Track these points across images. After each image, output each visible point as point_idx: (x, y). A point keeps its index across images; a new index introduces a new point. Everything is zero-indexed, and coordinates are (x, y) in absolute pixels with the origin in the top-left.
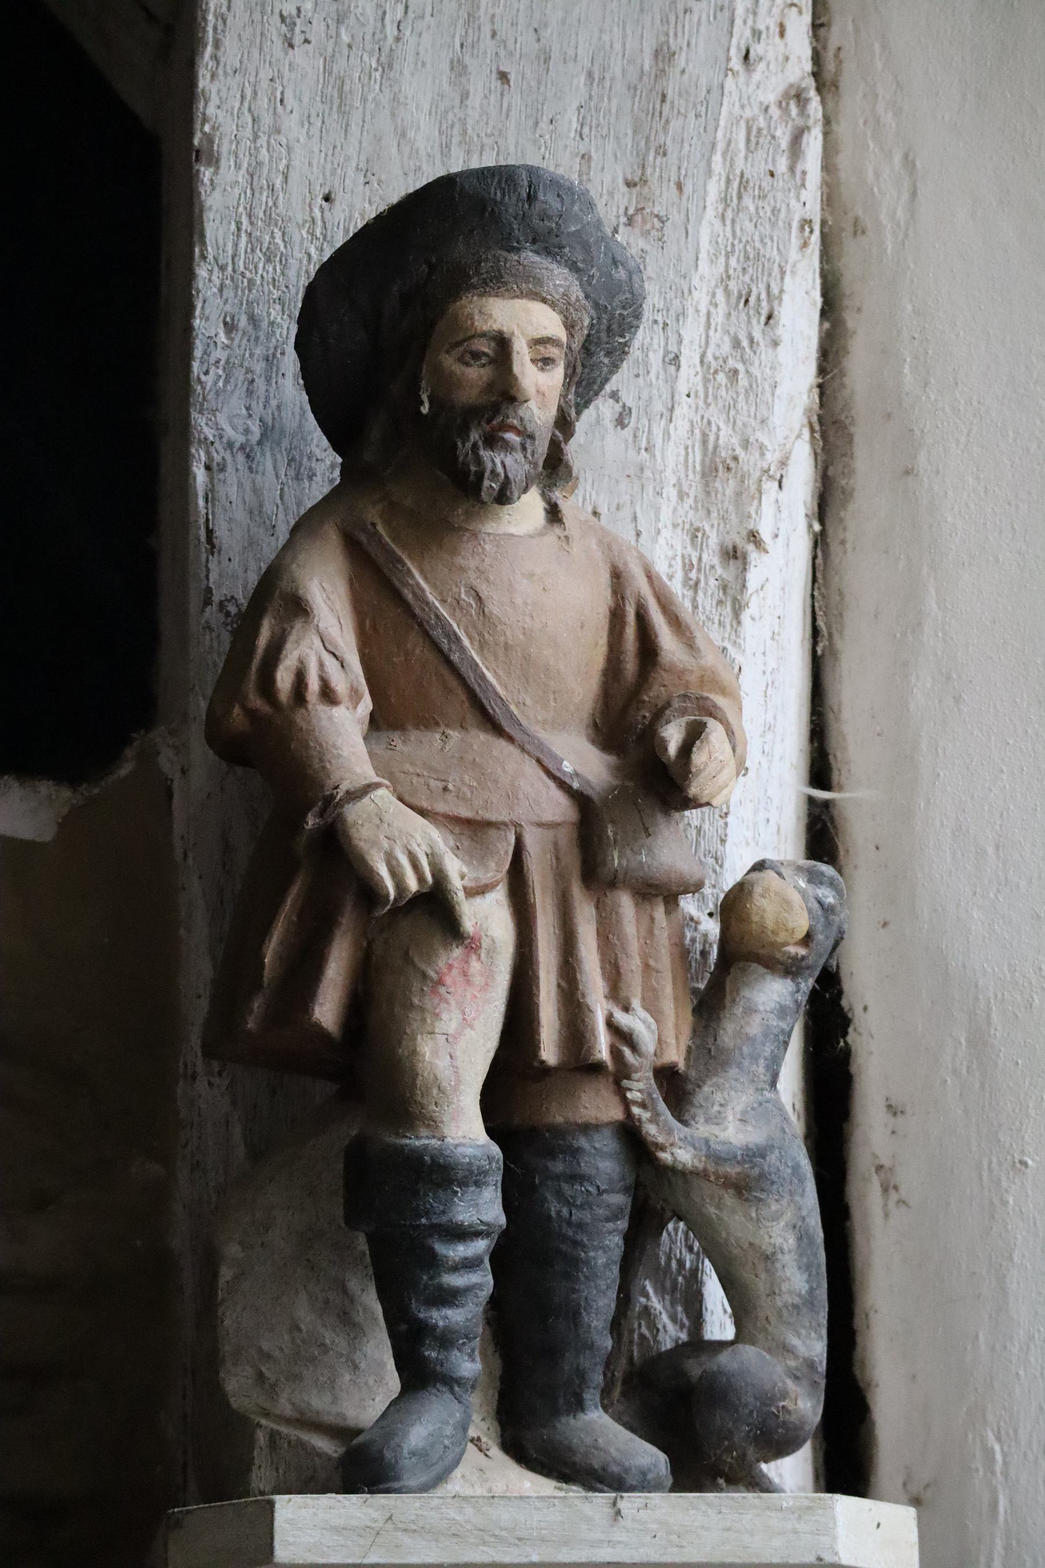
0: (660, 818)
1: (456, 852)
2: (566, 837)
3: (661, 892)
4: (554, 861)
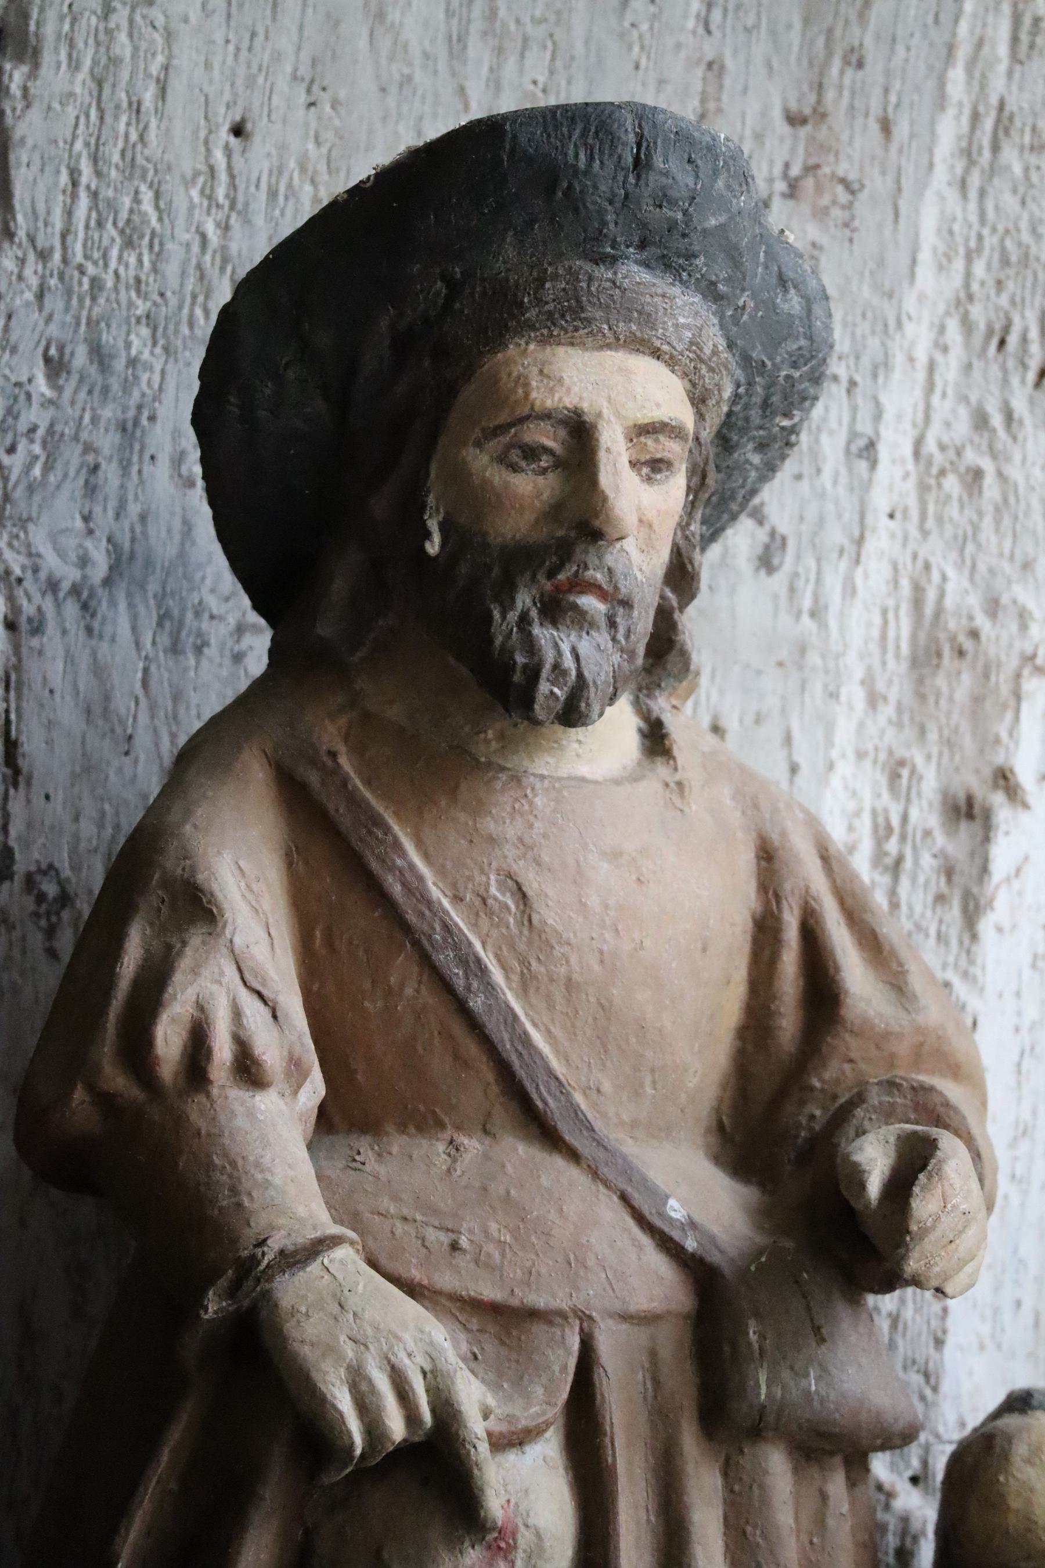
0: (842, 1309)
1: (473, 1365)
2: (670, 1341)
3: (838, 1446)
4: (649, 1385)
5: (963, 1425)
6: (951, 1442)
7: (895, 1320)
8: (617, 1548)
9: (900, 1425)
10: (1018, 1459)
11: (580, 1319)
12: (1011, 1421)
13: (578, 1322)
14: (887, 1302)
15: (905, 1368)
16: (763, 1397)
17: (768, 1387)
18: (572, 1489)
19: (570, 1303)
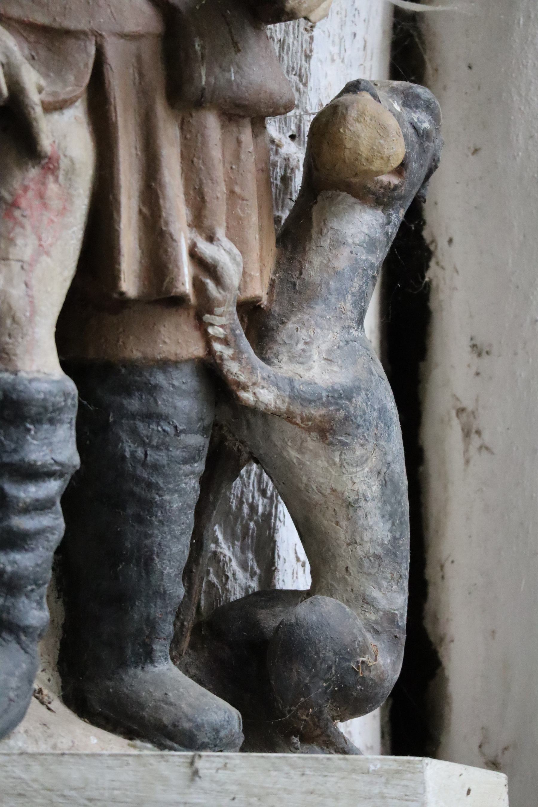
0: (250, 32)
1: (32, 62)
2: (149, 50)
3: (249, 113)
4: (137, 76)
5: (322, 105)
6: (314, 114)
7: (282, 43)
8: (118, 169)
9: (282, 102)
10: (351, 119)
11: (96, 36)
12: (349, 97)
13: (94, 38)
14: (276, 30)
15: (288, 72)
16: (203, 83)
17: (207, 78)
18: (92, 135)
19: (89, 27)
